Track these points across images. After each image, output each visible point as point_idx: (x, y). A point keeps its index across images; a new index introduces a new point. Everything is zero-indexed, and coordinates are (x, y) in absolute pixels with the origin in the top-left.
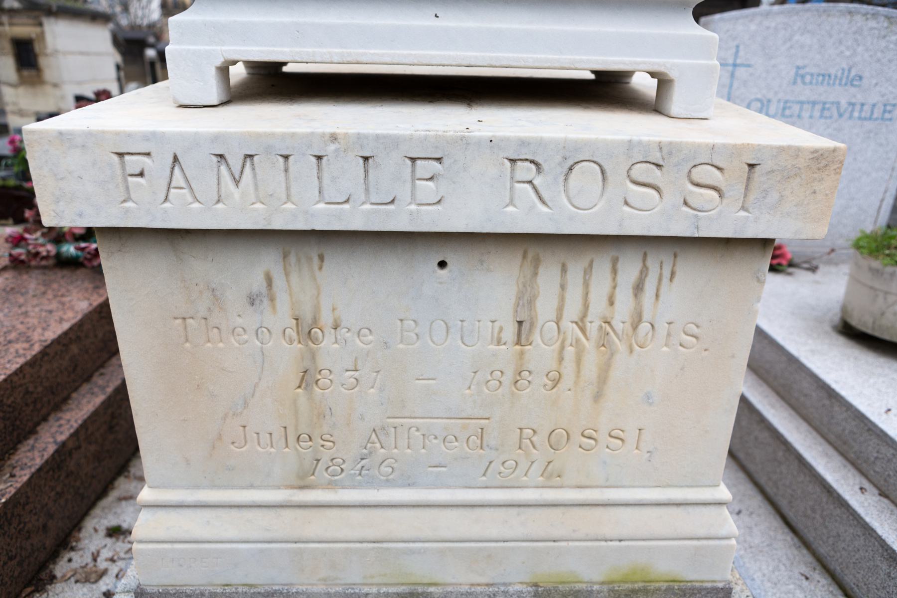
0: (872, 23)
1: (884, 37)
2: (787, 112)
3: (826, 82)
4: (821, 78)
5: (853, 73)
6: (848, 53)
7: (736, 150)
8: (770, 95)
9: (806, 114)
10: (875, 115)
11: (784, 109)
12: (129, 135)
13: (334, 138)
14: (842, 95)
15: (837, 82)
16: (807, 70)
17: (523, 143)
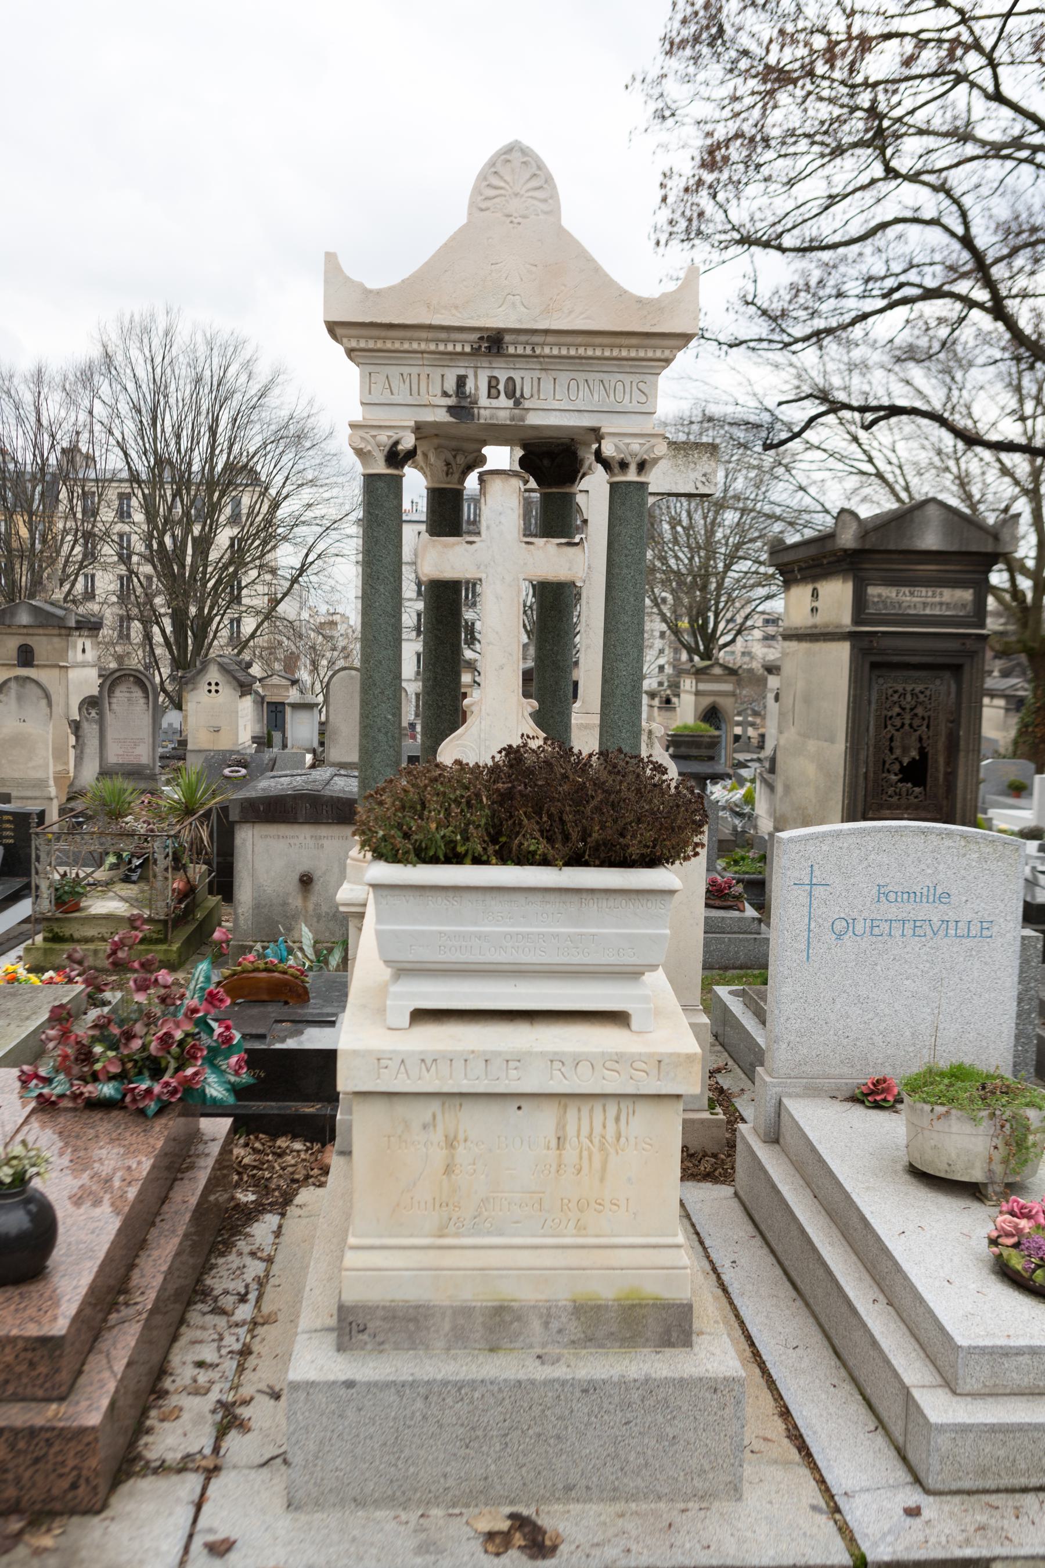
0: (948, 843)
1: (964, 855)
2: (876, 931)
3: (912, 900)
4: (906, 896)
5: (939, 891)
6: (929, 871)
7: (651, 1055)
8: (855, 915)
9: (897, 933)
10: (973, 933)
11: (872, 927)
12: (383, 1052)
13: (473, 1052)
14: (934, 913)
15: (924, 900)
16: (890, 888)
17: (556, 1053)
